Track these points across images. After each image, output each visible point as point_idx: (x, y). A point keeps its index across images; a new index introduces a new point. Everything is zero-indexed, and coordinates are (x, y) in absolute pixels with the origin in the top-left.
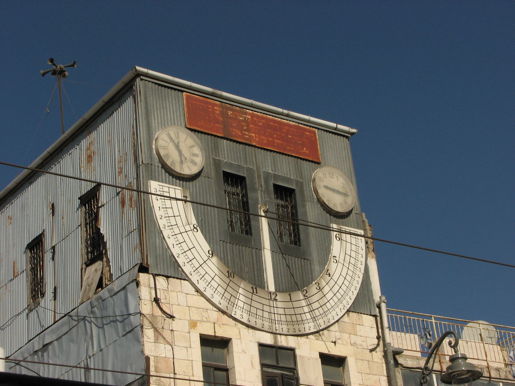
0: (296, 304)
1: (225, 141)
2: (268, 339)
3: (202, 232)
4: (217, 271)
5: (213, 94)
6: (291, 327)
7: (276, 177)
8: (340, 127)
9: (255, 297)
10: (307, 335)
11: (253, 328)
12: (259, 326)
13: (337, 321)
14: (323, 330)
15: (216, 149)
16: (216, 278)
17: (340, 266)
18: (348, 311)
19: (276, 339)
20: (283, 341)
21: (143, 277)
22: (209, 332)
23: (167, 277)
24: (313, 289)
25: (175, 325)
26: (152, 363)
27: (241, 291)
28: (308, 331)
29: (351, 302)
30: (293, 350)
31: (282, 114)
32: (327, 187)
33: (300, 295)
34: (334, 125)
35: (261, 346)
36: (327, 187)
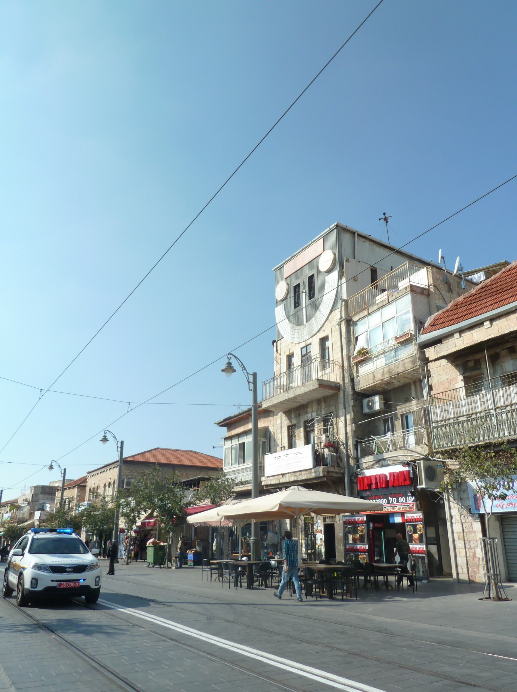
2: (303, 344)
5: (292, 257)
8: (331, 227)
9: (300, 331)
10: (316, 334)
13: (326, 320)
14: (321, 328)
16: (290, 332)
18: (331, 312)
20: (308, 342)
21: (275, 344)
22: (288, 353)
27: (296, 331)
29: (330, 308)
30: (310, 344)
31: (312, 243)
33: (313, 319)
34: (329, 229)
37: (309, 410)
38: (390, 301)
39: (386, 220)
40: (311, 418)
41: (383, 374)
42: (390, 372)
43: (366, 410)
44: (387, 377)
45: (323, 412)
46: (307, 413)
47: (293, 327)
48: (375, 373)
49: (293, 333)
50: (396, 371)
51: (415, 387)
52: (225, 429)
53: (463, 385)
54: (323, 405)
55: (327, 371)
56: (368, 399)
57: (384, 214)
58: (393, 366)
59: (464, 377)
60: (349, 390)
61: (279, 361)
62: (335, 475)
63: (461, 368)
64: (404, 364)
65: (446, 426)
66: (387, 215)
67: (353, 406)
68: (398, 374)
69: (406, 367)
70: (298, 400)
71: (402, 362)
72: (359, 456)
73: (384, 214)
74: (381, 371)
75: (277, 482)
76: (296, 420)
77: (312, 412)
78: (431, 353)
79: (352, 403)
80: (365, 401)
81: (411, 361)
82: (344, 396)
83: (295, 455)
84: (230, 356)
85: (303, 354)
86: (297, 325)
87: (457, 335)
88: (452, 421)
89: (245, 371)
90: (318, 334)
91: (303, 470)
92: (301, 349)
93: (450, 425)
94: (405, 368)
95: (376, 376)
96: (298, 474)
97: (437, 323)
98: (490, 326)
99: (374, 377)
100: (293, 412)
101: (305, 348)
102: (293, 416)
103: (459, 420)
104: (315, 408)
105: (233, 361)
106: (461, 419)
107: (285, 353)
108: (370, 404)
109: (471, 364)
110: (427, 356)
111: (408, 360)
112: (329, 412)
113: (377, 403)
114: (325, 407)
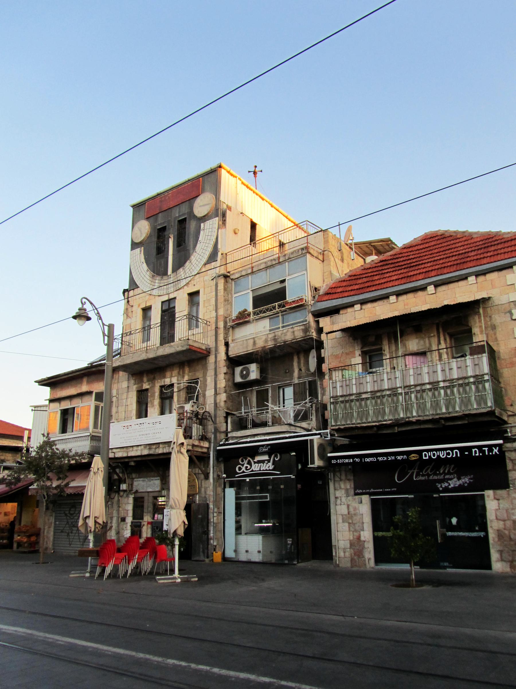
0: (178, 276)
1: (160, 214)
2: (166, 298)
3: (146, 263)
4: (148, 277)
6: (175, 288)
7: (180, 216)
9: (162, 281)
11: (161, 296)
12: (162, 294)
15: (156, 220)
16: (148, 281)
17: (202, 243)
18: (205, 264)
19: (169, 297)
20: (172, 296)
21: (126, 294)
22: (143, 306)
23: (133, 289)
24: (187, 263)
25: (134, 309)
26: (124, 328)
27: (157, 281)
28: (182, 286)
30: (175, 298)
32: (200, 206)
33: (181, 269)
35: (163, 302)
36: (200, 206)
37: (168, 374)
38: (281, 260)
39: (255, 173)
40: (169, 383)
41: (266, 341)
42: (275, 339)
43: (238, 379)
44: (270, 344)
45: (186, 378)
46: (165, 377)
47: (153, 276)
48: (256, 339)
49: (153, 283)
50: (283, 339)
51: (299, 358)
52: (48, 389)
53: (361, 362)
54: (187, 370)
55: (195, 331)
56: (240, 368)
57: (256, 167)
58: (279, 333)
59: (362, 352)
60: (222, 356)
61: (130, 314)
62: (200, 450)
63: (359, 342)
64: (294, 332)
65: (347, 401)
66: (257, 170)
67: (225, 373)
68: (285, 342)
69: (296, 335)
70: (156, 362)
71: (292, 330)
72: (229, 430)
73: (256, 167)
74: (264, 338)
75: (125, 455)
76: (149, 384)
77: (171, 377)
78: (325, 322)
79: (224, 370)
80: (238, 370)
81: (302, 329)
82: (216, 362)
83: (151, 425)
84: (84, 300)
85: (164, 309)
86: (158, 274)
87: (357, 307)
88: (353, 397)
89: (100, 321)
90: (186, 287)
91: (162, 443)
92: (163, 302)
93: (352, 401)
94: (295, 337)
95: (257, 341)
96: (154, 447)
97: (333, 291)
98: (395, 301)
99: (254, 343)
100: (145, 375)
101: (167, 303)
102: (145, 379)
103: (361, 397)
104: (175, 372)
105: (88, 307)
106: (364, 396)
107: (139, 305)
108: (245, 373)
109: (372, 339)
110: (321, 326)
111: (298, 328)
112: (194, 378)
113: (254, 372)
114: (190, 372)
